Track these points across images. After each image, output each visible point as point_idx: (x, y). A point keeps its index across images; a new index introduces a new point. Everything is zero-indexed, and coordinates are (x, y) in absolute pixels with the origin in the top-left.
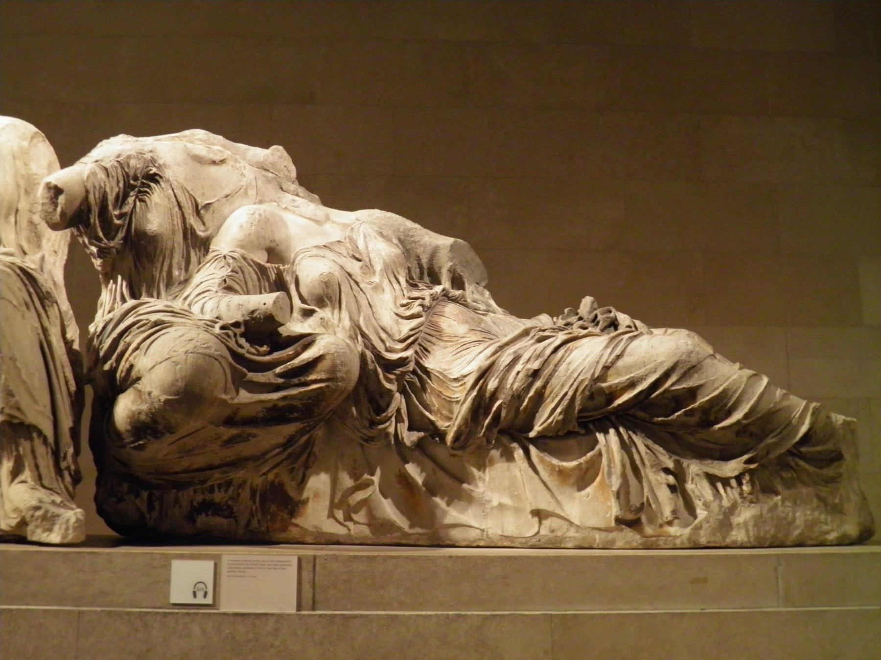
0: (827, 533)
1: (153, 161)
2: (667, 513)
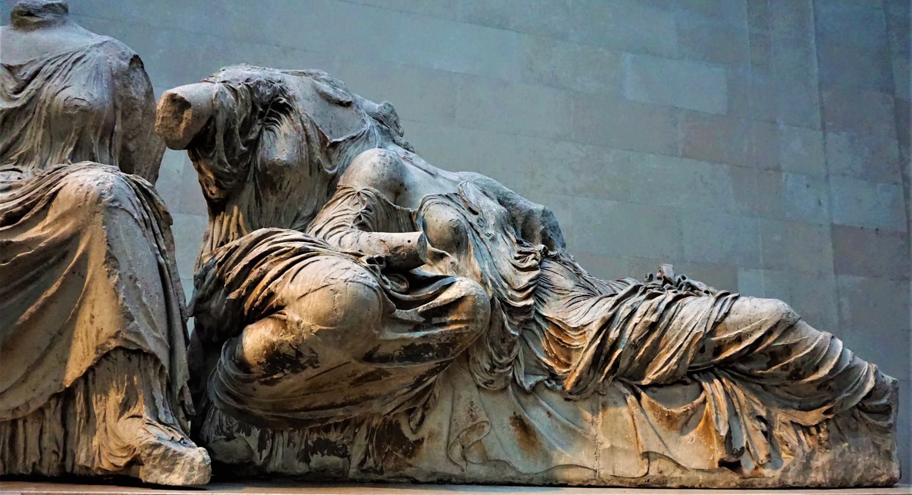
1: (283, 91)
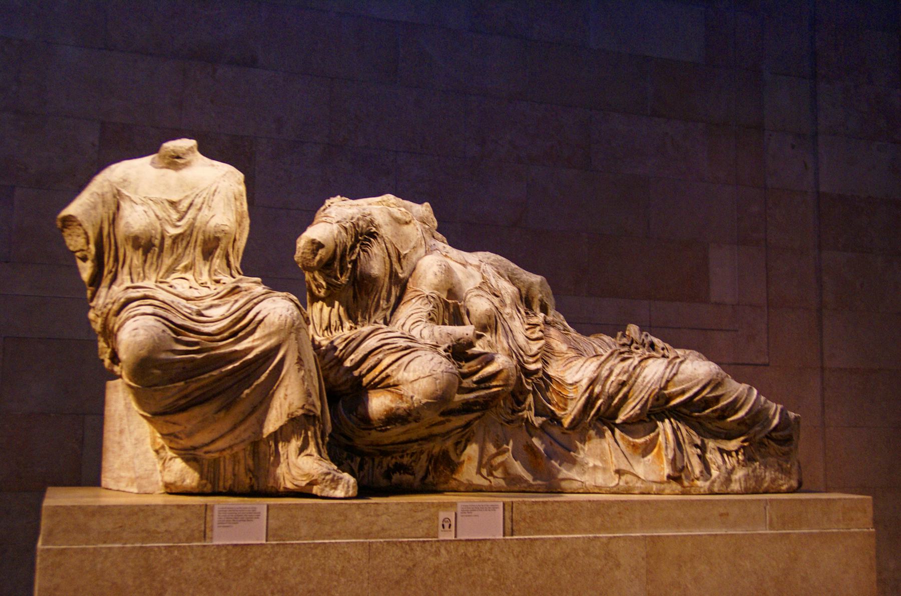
0: (782, 485)
1: (372, 222)
2: (697, 471)
